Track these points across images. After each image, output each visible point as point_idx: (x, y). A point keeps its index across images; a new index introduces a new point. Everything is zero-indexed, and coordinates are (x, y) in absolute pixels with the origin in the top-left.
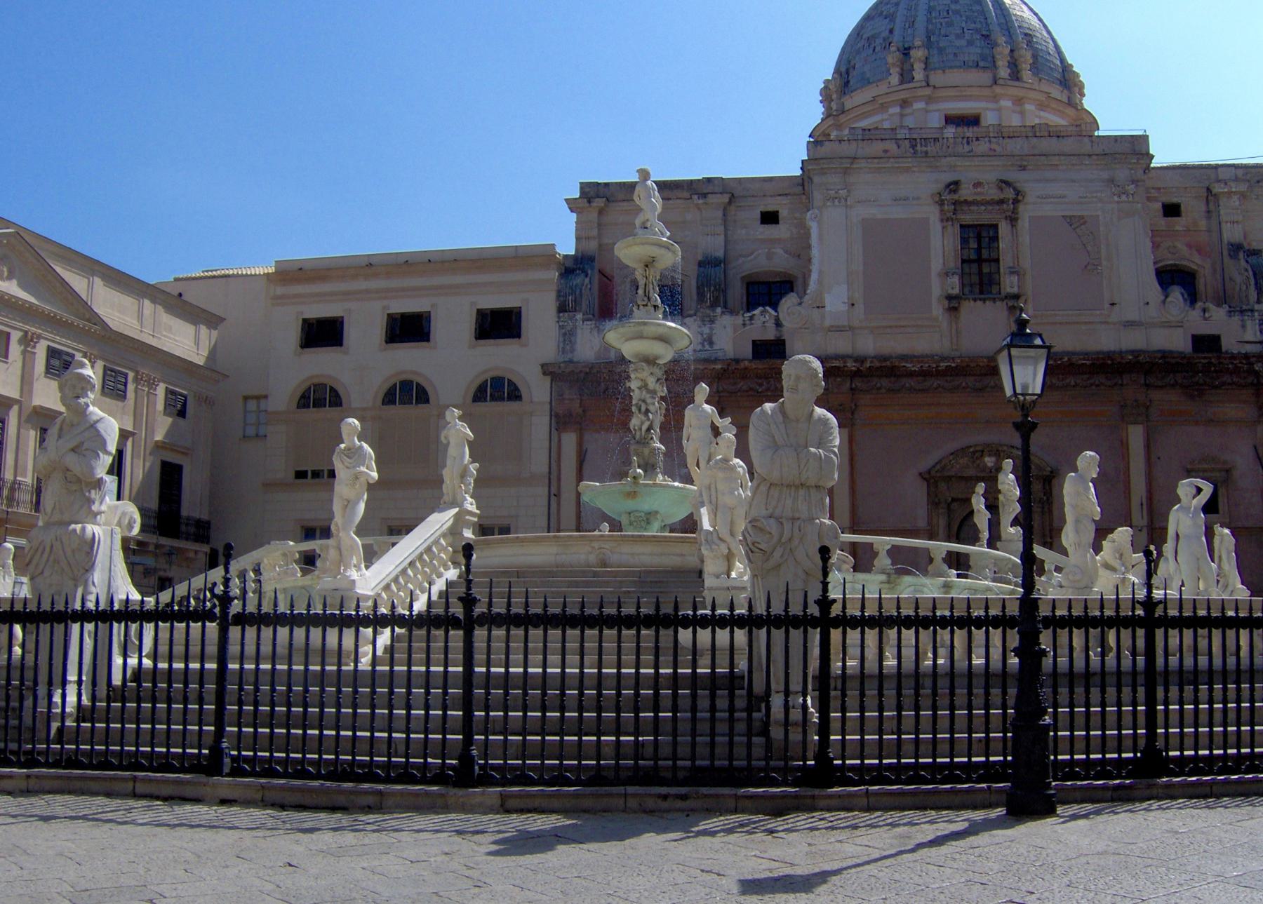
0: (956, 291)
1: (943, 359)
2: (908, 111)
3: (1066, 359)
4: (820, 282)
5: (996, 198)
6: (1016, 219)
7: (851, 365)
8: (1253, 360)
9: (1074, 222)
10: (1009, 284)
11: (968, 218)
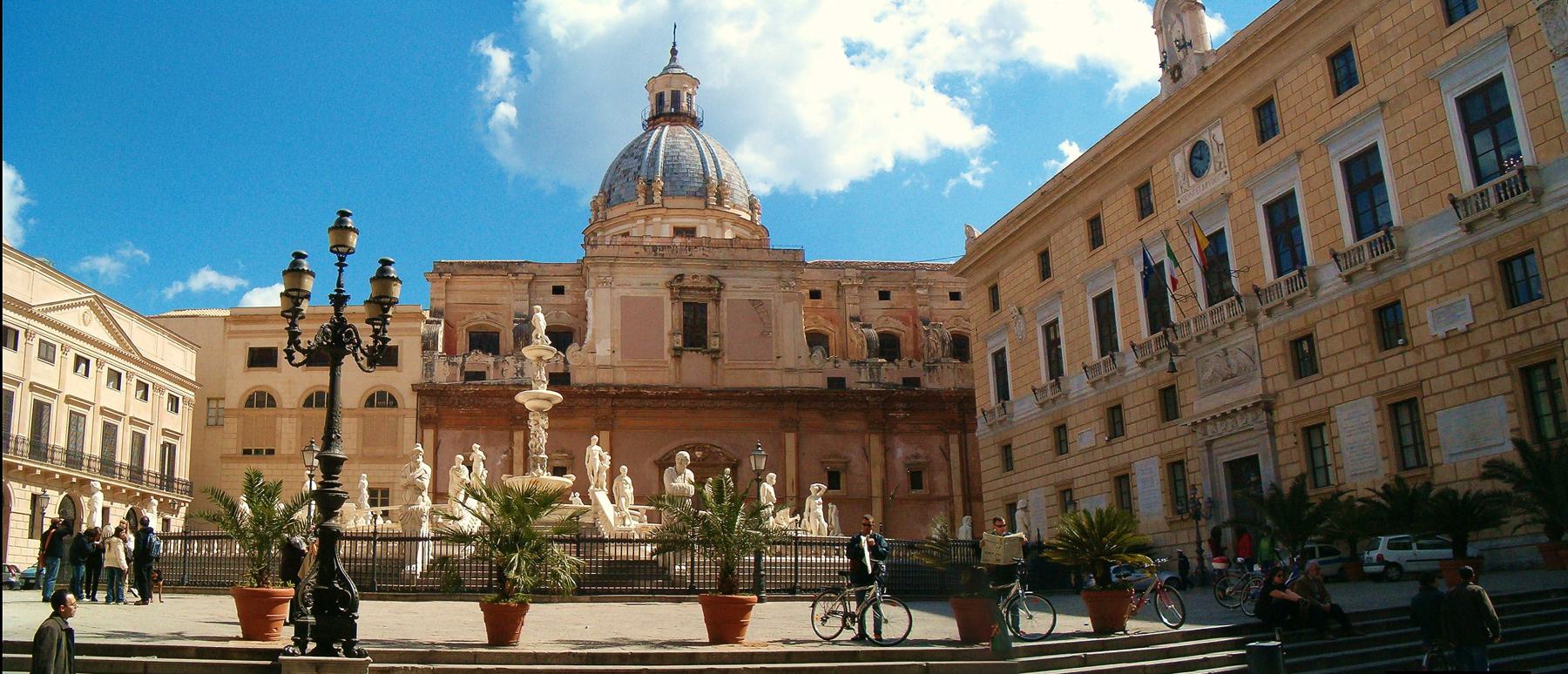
0: (680, 345)
1: (670, 388)
3: (748, 393)
7: (613, 391)
8: (865, 394)
10: (714, 343)
11: (688, 298)
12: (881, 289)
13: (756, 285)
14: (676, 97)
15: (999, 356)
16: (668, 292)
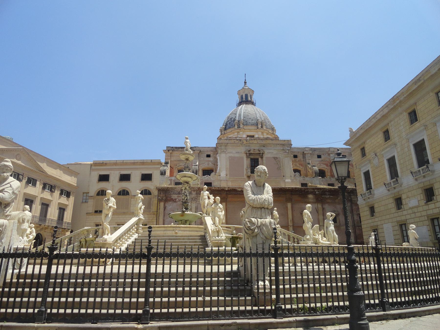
2: (238, 134)
4: (220, 170)
5: (258, 153)
6: (263, 157)
9: (275, 158)
11: (252, 157)
12: (318, 155)
13: (275, 152)
14: (246, 96)
15: (367, 175)
16: (245, 155)
